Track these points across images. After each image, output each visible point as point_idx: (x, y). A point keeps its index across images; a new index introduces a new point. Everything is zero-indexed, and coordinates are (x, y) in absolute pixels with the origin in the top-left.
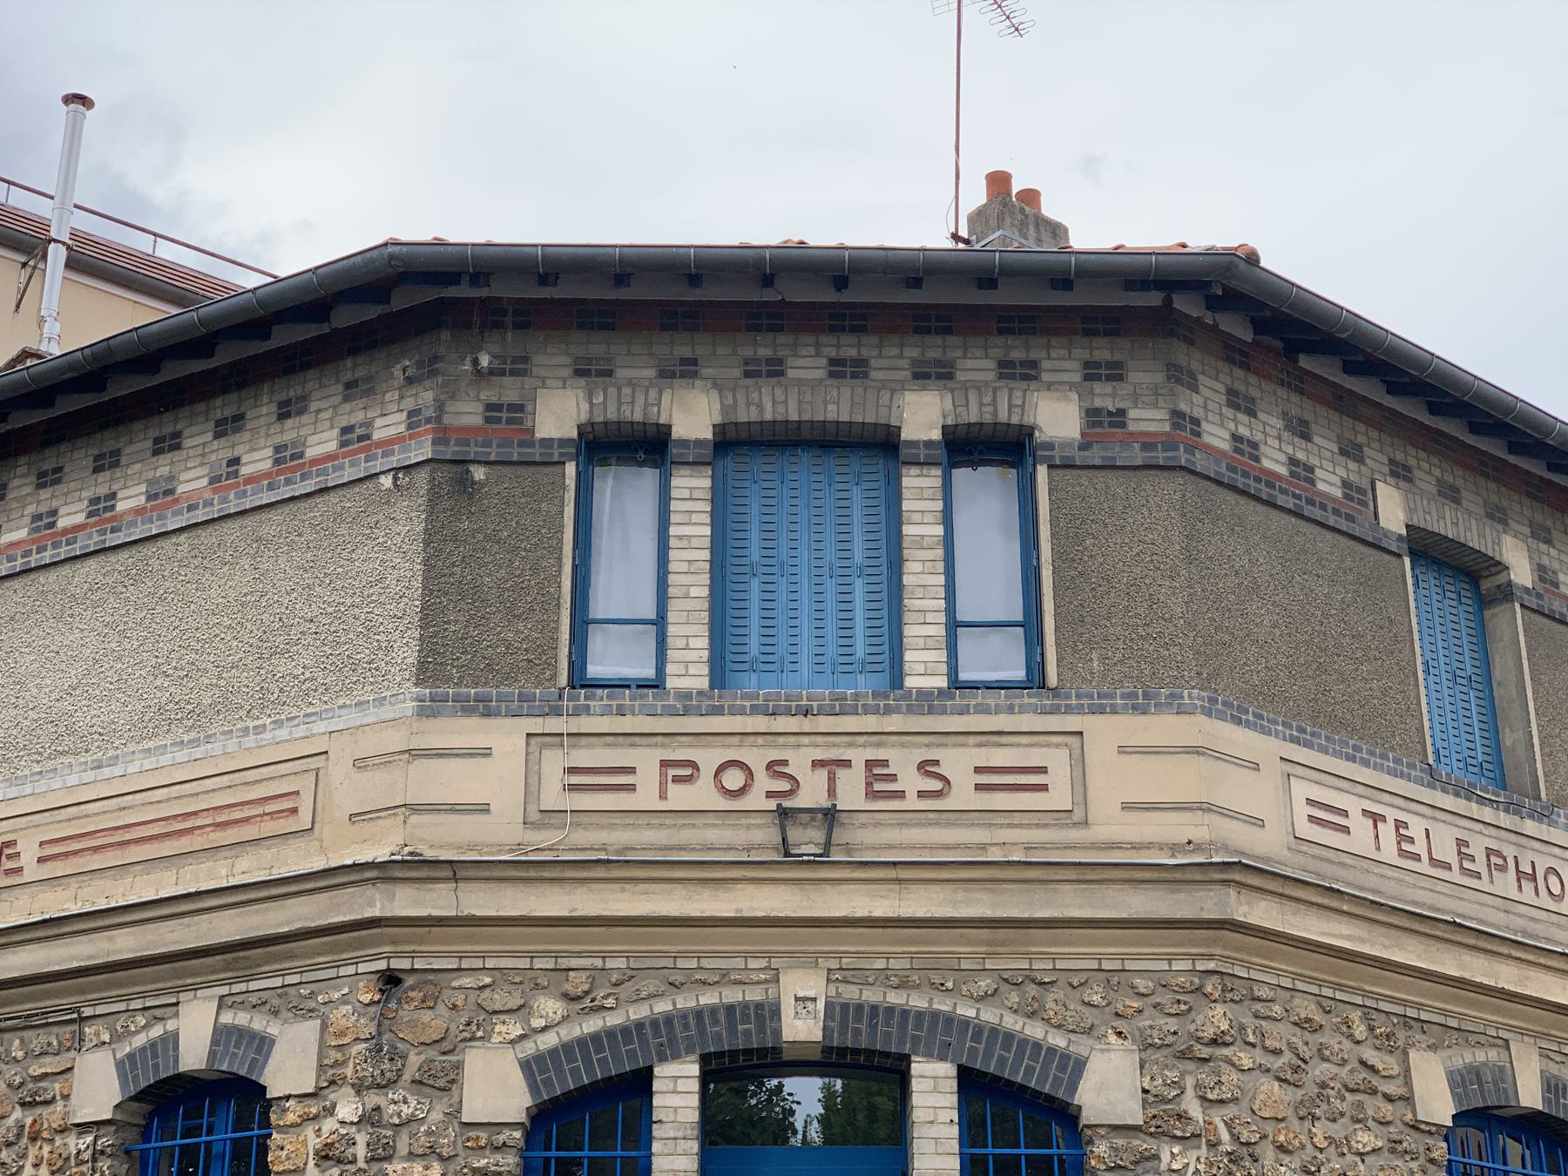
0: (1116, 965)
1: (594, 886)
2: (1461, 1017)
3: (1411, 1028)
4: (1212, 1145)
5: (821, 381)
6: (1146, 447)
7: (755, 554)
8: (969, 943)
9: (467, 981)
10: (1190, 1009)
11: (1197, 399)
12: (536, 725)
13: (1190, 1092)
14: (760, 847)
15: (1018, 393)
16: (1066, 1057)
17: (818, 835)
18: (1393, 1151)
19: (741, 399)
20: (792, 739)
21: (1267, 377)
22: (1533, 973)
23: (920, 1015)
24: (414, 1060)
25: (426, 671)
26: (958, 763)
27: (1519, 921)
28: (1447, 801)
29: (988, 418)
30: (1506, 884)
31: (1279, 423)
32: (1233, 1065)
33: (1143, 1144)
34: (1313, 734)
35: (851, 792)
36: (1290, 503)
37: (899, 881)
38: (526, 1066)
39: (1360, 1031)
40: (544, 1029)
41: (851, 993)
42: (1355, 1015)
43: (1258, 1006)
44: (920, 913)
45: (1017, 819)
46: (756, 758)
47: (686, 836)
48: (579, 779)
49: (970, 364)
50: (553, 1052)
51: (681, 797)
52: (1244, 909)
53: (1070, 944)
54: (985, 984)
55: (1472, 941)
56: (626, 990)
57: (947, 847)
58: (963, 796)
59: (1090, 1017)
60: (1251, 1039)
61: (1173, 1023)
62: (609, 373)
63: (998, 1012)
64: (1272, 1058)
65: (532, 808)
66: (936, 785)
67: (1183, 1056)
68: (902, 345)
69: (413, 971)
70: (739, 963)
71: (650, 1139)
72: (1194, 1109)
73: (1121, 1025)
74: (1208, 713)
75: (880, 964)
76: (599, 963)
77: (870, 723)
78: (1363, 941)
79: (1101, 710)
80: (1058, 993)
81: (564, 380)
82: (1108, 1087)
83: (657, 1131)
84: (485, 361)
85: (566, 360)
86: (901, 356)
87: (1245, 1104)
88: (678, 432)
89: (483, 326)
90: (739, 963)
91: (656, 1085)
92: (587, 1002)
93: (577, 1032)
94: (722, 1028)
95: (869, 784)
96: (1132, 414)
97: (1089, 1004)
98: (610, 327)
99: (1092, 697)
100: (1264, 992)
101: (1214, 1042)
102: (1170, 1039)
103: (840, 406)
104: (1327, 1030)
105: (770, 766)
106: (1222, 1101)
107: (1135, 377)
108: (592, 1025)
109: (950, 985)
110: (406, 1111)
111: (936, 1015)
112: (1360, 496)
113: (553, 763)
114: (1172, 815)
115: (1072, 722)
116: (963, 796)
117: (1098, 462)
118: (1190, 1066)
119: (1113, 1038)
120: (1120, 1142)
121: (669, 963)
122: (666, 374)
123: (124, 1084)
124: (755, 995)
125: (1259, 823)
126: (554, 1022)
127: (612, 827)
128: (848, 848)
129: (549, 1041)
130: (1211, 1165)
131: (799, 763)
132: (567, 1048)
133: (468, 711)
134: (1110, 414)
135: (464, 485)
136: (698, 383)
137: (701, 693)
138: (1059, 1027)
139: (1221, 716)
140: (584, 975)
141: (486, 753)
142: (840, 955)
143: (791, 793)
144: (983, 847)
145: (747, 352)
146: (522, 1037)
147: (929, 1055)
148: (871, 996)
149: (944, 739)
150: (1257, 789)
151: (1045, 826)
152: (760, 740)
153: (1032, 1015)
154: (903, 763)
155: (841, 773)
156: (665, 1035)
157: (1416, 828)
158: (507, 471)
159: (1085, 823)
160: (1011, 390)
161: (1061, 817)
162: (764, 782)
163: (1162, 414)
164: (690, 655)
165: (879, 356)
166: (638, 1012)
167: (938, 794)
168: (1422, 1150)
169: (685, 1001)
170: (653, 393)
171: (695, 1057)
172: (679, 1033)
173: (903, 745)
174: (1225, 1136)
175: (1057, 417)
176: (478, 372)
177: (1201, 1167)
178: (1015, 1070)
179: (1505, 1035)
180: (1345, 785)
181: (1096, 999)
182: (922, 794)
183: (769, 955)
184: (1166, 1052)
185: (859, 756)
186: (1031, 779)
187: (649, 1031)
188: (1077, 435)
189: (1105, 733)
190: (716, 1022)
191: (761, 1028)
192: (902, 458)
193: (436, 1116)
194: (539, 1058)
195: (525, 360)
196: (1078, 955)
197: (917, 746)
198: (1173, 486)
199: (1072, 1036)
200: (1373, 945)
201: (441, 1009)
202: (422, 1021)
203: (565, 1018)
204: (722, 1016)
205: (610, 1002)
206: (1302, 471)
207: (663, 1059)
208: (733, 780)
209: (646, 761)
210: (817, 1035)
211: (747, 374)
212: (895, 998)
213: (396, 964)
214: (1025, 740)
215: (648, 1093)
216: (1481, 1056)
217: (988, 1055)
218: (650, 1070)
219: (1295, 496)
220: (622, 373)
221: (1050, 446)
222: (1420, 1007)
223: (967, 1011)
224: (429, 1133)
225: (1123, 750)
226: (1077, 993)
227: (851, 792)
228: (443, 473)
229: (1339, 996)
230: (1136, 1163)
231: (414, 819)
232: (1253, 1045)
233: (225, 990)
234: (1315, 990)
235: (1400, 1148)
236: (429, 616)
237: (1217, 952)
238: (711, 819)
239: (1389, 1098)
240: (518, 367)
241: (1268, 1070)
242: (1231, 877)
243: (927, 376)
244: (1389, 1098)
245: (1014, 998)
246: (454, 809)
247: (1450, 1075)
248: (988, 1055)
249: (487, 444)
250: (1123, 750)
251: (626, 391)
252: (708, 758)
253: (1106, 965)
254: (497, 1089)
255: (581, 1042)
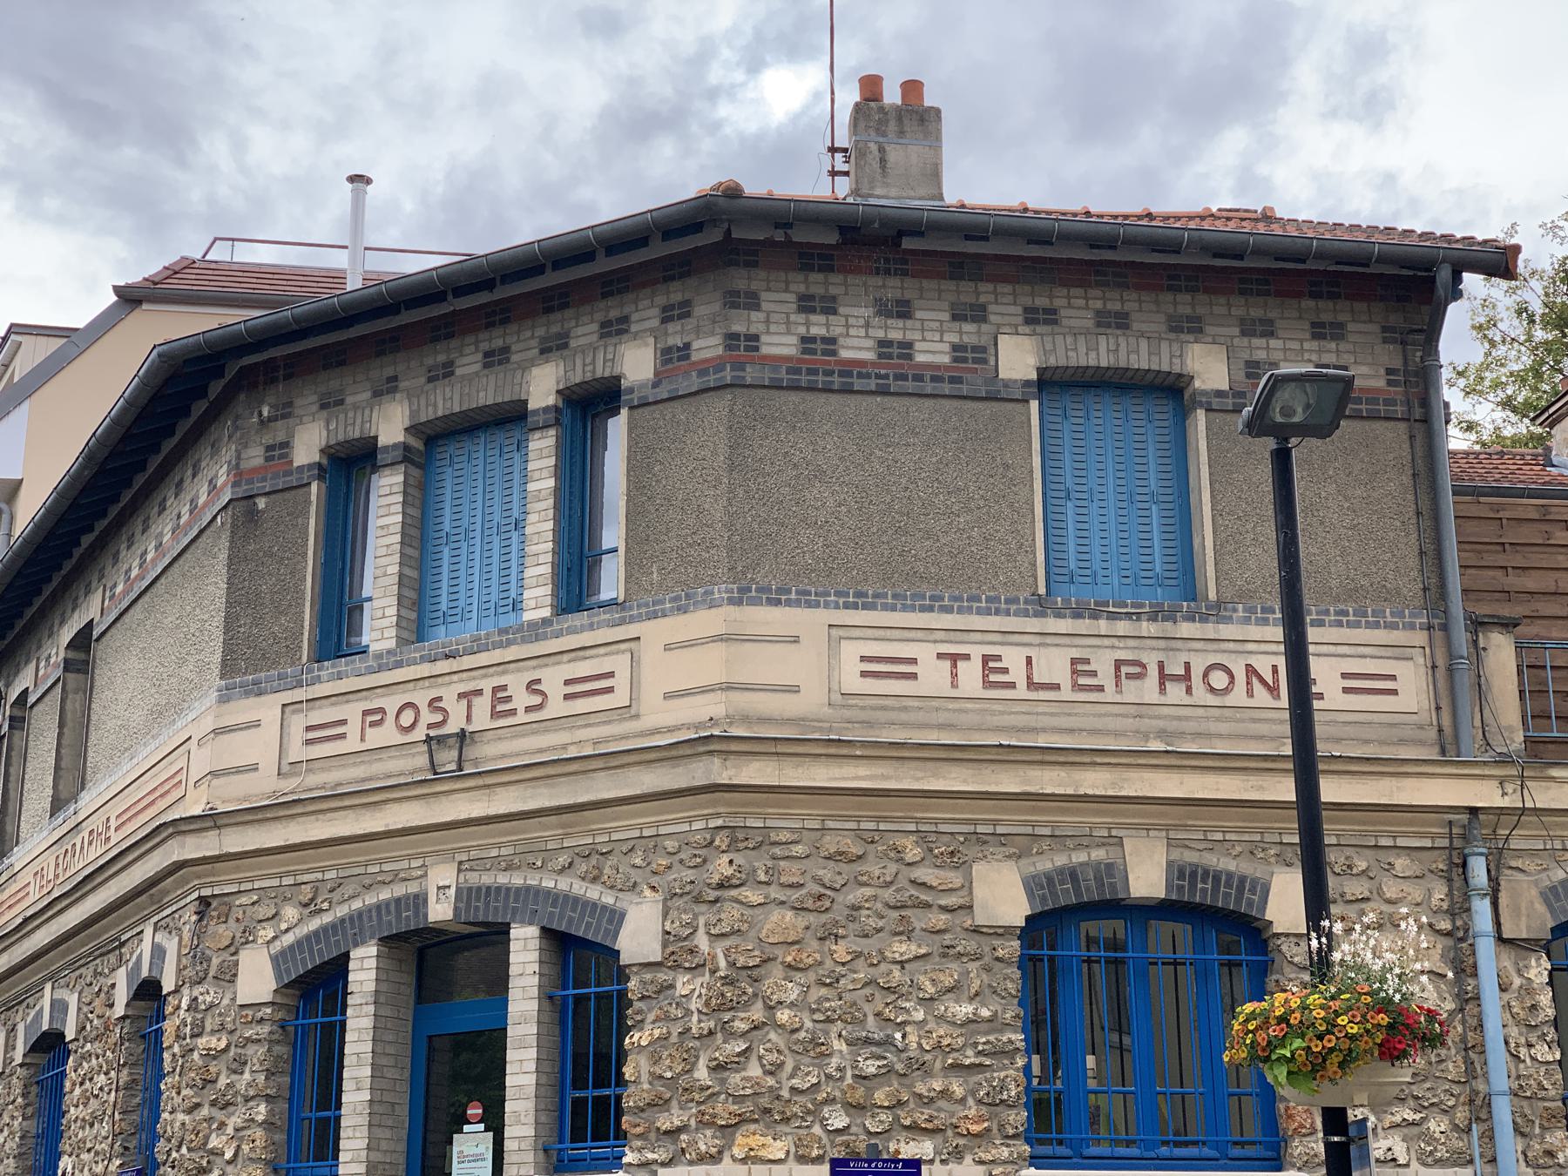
0: (652, 832)
1: (301, 819)
2: (1054, 825)
3: (985, 842)
4: (713, 972)
5: (477, 373)
6: (703, 373)
7: (447, 527)
8: (546, 828)
9: (244, 900)
10: (705, 861)
11: (755, 315)
12: (287, 697)
13: (701, 930)
14: (421, 770)
15: (611, 349)
16: (613, 912)
17: (455, 754)
18: (945, 955)
19: (423, 402)
20: (447, 678)
21: (857, 271)
22: (1133, 774)
23: (518, 890)
24: (215, 961)
25: (227, 668)
26: (553, 679)
27: (1154, 722)
28: (1064, 625)
29: (589, 376)
30: (1148, 689)
31: (867, 312)
32: (741, 903)
33: (662, 976)
34: (876, 596)
35: (482, 718)
36: (872, 384)
37: (488, 786)
38: (276, 960)
39: (913, 852)
40: (287, 930)
41: (474, 879)
42: (908, 842)
43: (777, 851)
44: (502, 810)
45: (593, 719)
46: (421, 698)
47: (378, 768)
48: (317, 733)
49: (580, 331)
50: (291, 947)
51: (376, 738)
52: (732, 772)
53: (615, 819)
54: (563, 859)
55: (1039, 758)
56: (336, 896)
57: (541, 751)
58: (556, 707)
59: (636, 876)
60: (763, 877)
61: (689, 875)
62: (341, 402)
63: (569, 880)
64: (789, 892)
65: (284, 762)
66: (537, 700)
67: (698, 900)
68: (533, 327)
69: (214, 896)
70: (405, 864)
71: (345, 1006)
72: (702, 942)
73: (654, 881)
74: (736, 602)
75: (494, 853)
76: (320, 876)
77: (496, 656)
78: (885, 777)
79: (653, 616)
80: (612, 860)
81: (313, 414)
82: (639, 936)
83: (350, 1000)
84: (265, 413)
85: (314, 398)
86: (533, 337)
87: (752, 934)
88: (383, 441)
89: (265, 383)
90: (405, 864)
91: (352, 965)
92: (312, 908)
93: (305, 931)
94: (392, 918)
95: (493, 707)
96: (695, 345)
97: (634, 866)
98: (341, 363)
99: (647, 605)
100: (784, 836)
101: (721, 886)
102: (688, 888)
103: (487, 393)
104: (871, 857)
105: (528, 686)
106: (723, 935)
107: (701, 310)
108: (315, 924)
109: (539, 863)
110: (209, 999)
111: (528, 888)
112: (975, 356)
113: (298, 723)
114: (699, 697)
115: (631, 630)
116: (556, 707)
117: (665, 396)
118: (703, 908)
119: (648, 892)
120: (648, 976)
121: (361, 870)
122: (377, 394)
123: (278, 976)
124: (413, 888)
125: (794, 689)
126: (295, 925)
127: (329, 769)
128: (476, 762)
129: (288, 939)
130: (709, 989)
131: (449, 695)
132: (299, 943)
133: (247, 694)
134: (679, 349)
135: (252, 516)
136: (398, 396)
137: (389, 652)
138: (612, 887)
139: (754, 602)
140: (308, 887)
141: (256, 724)
142: (468, 849)
143: (444, 722)
144: (564, 747)
145: (430, 361)
146: (275, 938)
147: (522, 922)
148: (487, 879)
149: (546, 660)
150: (800, 661)
151: (610, 722)
152: (427, 683)
153: (595, 880)
154: (516, 683)
155: (477, 701)
156: (354, 929)
157: (1013, 659)
158: (279, 496)
159: (637, 716)
160: (605, 347)
161: (627, 711)
162: (428, 717)
163: (716, 340)
164: (385, 622)
165: (518, 341)
166: (342, 911)
167: (540, 707)
168: (987, 949)
169: (371, 899)
170: (367, 412)
171: (374, 941)
172: (367, 925)
173: (519, 670)
174: (722, 963)
175: (636, 363)
176: (262, 422)
177: (704, 991)
178: (578, 929)
179: (1121, 833)
180: (920, 635)
181: (638, 861)
182: (528, 709)
183: (424, 855)
184: (686, 898)
185: (487, 685)
186: (600, 684)
187: (347, 924)
188: (651, 376)
189: (655, 632)
190: (389, 912)
191: (416, 914)
192: (530, 426)
193: (226, 1001)
194: (283, 953)
195: (290, 404)
196: (626, 826)
197: (527, 669)
198: (721, 405)
199: (620, 895)
200: (898, 779)
201: (231, 921)
202: (223, 932)
203: (300, 920)
204: (392, 908)
205: (325, 906)
206: (895, 352)
207: (356, 945)
208: (407, 718)
209: (352, 712)
210: (450, 915)
211: (430, 380)
212: (503, 879)
213: (206, 892)
214: (602, 650)
215: (346, 972)
216: (1080, 857)
217: (561, 917)
218: (345, 957)
219: (878, 376)
220: (349, 400)
221: (631, 390)
222: (995, 823)
223: (548, 883)
224: (220, 1014)
225: (668, 648)
226: (627, 858)
227: (482, 718)
228: (240, 506)
229: (882, 827)
230: (658, 992)
231: (216, 782)
232: (768, 884)
233: (156, 919)
234: (853, 825)
235: (952, 952)
236: (229, 625)
237: (721, 810)
238: (393, 753)
239: (945, 909)
240: (285, 412)
241: (783, 903)
242: (712, 748)
243: (549, 350)
244: (945, 909)
245: (583, 867)
246: (238, 771)
247: (1170, 864)
248: (561, 917)
249: (264, 479)
250: (668, 648)
251: (351, 414)
252: (391, 703)
253: (646, 833)
254: (257, 980)
255: (308, 937)
